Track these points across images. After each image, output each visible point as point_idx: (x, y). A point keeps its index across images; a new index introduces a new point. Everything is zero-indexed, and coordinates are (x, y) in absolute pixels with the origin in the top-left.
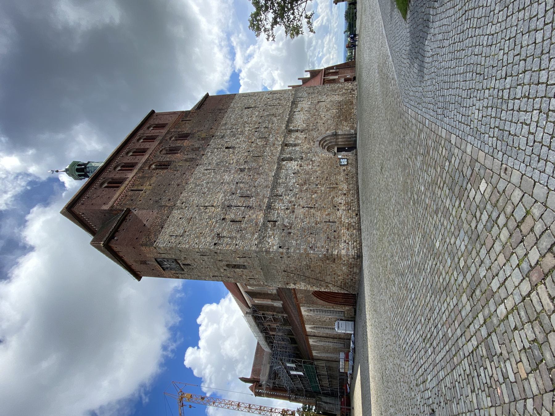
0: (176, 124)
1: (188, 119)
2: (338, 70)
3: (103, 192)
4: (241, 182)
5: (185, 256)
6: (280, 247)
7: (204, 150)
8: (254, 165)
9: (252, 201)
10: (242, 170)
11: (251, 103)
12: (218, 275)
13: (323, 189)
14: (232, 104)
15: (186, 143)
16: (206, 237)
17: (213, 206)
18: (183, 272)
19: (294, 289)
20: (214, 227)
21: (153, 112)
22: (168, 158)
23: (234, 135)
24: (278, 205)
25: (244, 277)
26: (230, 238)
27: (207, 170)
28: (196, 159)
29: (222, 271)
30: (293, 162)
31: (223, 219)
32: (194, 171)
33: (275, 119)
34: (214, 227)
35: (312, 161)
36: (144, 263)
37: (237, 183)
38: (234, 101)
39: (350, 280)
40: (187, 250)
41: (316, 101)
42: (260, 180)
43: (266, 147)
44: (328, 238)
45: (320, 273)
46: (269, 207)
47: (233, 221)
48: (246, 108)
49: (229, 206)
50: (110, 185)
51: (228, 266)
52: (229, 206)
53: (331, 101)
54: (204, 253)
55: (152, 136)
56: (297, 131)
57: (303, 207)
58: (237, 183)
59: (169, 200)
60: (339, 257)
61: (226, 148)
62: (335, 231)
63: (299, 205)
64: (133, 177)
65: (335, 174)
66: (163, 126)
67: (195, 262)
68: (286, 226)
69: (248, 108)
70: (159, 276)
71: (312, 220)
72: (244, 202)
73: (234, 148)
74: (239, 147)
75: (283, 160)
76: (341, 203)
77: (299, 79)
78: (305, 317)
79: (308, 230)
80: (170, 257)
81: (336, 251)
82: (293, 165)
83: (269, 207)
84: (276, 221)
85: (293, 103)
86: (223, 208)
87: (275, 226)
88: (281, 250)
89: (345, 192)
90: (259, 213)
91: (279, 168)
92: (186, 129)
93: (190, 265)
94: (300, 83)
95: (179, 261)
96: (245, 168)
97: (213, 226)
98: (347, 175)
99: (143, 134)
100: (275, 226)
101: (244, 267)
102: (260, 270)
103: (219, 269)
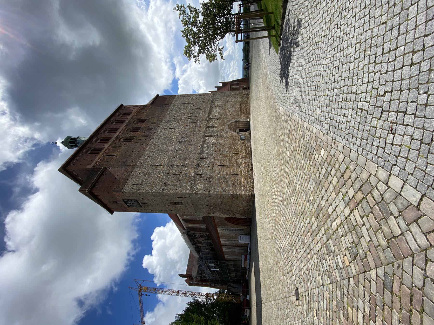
0: (137, 113)
1: (145, 110)
2: (239, 83)
3: (88, 156)
4: (180, 150)
5: (143, 198)
6: (204, 191)
7: (155, 129)
8: (188, 139)
9: (187, 162)
10: (180, 143)
12: (165, 209)
13: (231, 154)
14: (174, 101)
15: (144, 125)
16: (156, 185)
17: (161, 165)
18: (141, 208)
19: (213, 217)
20: (162, 178)
21: (122, 105)
22: (131, 134)
23: (175, 121)
24: (203, 164)
25: (182, 210)
26: (173, 185)
27: (157, 142)
28: (151, 135)
29: (167, 206)
30: (212, 138)
31: (168, 173)
32: (149, 143)
33: (201, 111)
34: (162, 178)
35: (224, 137)
36: (115, 202)
37: (177, 150)
38: (175, 99)
39: (247, 210)
40: (144, 194)
42: (192, 149)
43: (195, 128)
44: (234, 184)
45: (229, 206)
46: (198, 165)
47: (174, 175)
48: (182, 104)
49: (172, 165)
50: (93, 152)
51: (171, 203)
52: (172, 165)
54: (155, 195)
55: (121, 120)
56: (214, 119)
57: (219, 166)
58: (177, 150)
59: (133, 161)
60: (241, 196)
61: (170, 128)
62: (238, 180)
63: (216, 164)
64: (108, 147)
65: (238, 146)
67: (150, 201)
68: (208, 177)
69: (184, 104)
70: (125, 211)
71: (224, 173)
72: (181, 162)
73: (175, 128)
74: (178, 128)
75: (206, 136)
76: (241, 163)
77: (215, 87)
78: (220, 234)
79: (222, 180)
80: (132, 198)
81: (239, 192)
82: (213, 140)
83: (198, 165)
84: (202, 174)
86: (168, 167)
87: (201, 177)
88: (205, 192)
89: (243, 156)
90: (191, 169)
91: (204, 142)
92: (144, 116)
93: (146, 203)
94: (216, 89)
95: (139, 201)
96: (182, 141)
97: (161, 178)
98: (245, 146)
99: (115, 119)
100: (201, 177)
101: (182, 204)
102: (191, 205)
103: (165, 206)
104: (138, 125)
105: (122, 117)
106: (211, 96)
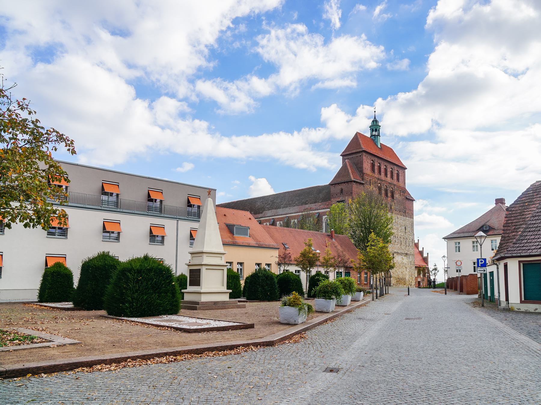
0: (399, 187)
2: (426, 277)
11: (408, 229)
14: (407, 218)
15: (389, 199)
33: (399, 245)
41: (407, 267)
53: (406, 274)
66: (398, 179)
85: (407, 254)
94: (420, 249)
104: (389, 194)
105: (395, 175)
106: (411, 253)
